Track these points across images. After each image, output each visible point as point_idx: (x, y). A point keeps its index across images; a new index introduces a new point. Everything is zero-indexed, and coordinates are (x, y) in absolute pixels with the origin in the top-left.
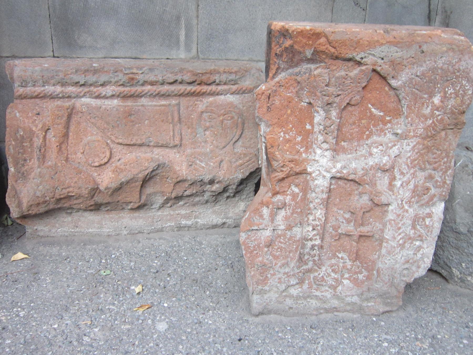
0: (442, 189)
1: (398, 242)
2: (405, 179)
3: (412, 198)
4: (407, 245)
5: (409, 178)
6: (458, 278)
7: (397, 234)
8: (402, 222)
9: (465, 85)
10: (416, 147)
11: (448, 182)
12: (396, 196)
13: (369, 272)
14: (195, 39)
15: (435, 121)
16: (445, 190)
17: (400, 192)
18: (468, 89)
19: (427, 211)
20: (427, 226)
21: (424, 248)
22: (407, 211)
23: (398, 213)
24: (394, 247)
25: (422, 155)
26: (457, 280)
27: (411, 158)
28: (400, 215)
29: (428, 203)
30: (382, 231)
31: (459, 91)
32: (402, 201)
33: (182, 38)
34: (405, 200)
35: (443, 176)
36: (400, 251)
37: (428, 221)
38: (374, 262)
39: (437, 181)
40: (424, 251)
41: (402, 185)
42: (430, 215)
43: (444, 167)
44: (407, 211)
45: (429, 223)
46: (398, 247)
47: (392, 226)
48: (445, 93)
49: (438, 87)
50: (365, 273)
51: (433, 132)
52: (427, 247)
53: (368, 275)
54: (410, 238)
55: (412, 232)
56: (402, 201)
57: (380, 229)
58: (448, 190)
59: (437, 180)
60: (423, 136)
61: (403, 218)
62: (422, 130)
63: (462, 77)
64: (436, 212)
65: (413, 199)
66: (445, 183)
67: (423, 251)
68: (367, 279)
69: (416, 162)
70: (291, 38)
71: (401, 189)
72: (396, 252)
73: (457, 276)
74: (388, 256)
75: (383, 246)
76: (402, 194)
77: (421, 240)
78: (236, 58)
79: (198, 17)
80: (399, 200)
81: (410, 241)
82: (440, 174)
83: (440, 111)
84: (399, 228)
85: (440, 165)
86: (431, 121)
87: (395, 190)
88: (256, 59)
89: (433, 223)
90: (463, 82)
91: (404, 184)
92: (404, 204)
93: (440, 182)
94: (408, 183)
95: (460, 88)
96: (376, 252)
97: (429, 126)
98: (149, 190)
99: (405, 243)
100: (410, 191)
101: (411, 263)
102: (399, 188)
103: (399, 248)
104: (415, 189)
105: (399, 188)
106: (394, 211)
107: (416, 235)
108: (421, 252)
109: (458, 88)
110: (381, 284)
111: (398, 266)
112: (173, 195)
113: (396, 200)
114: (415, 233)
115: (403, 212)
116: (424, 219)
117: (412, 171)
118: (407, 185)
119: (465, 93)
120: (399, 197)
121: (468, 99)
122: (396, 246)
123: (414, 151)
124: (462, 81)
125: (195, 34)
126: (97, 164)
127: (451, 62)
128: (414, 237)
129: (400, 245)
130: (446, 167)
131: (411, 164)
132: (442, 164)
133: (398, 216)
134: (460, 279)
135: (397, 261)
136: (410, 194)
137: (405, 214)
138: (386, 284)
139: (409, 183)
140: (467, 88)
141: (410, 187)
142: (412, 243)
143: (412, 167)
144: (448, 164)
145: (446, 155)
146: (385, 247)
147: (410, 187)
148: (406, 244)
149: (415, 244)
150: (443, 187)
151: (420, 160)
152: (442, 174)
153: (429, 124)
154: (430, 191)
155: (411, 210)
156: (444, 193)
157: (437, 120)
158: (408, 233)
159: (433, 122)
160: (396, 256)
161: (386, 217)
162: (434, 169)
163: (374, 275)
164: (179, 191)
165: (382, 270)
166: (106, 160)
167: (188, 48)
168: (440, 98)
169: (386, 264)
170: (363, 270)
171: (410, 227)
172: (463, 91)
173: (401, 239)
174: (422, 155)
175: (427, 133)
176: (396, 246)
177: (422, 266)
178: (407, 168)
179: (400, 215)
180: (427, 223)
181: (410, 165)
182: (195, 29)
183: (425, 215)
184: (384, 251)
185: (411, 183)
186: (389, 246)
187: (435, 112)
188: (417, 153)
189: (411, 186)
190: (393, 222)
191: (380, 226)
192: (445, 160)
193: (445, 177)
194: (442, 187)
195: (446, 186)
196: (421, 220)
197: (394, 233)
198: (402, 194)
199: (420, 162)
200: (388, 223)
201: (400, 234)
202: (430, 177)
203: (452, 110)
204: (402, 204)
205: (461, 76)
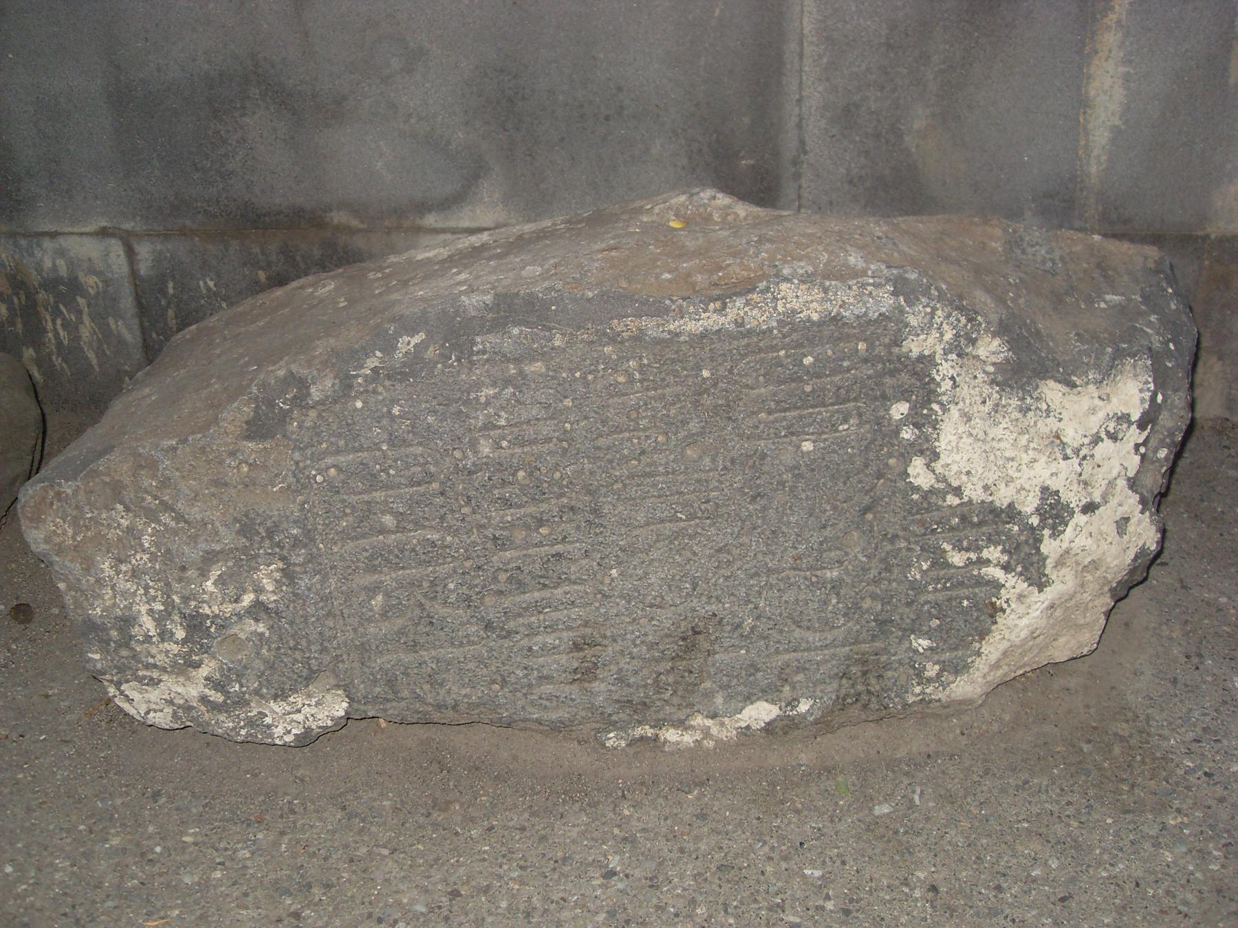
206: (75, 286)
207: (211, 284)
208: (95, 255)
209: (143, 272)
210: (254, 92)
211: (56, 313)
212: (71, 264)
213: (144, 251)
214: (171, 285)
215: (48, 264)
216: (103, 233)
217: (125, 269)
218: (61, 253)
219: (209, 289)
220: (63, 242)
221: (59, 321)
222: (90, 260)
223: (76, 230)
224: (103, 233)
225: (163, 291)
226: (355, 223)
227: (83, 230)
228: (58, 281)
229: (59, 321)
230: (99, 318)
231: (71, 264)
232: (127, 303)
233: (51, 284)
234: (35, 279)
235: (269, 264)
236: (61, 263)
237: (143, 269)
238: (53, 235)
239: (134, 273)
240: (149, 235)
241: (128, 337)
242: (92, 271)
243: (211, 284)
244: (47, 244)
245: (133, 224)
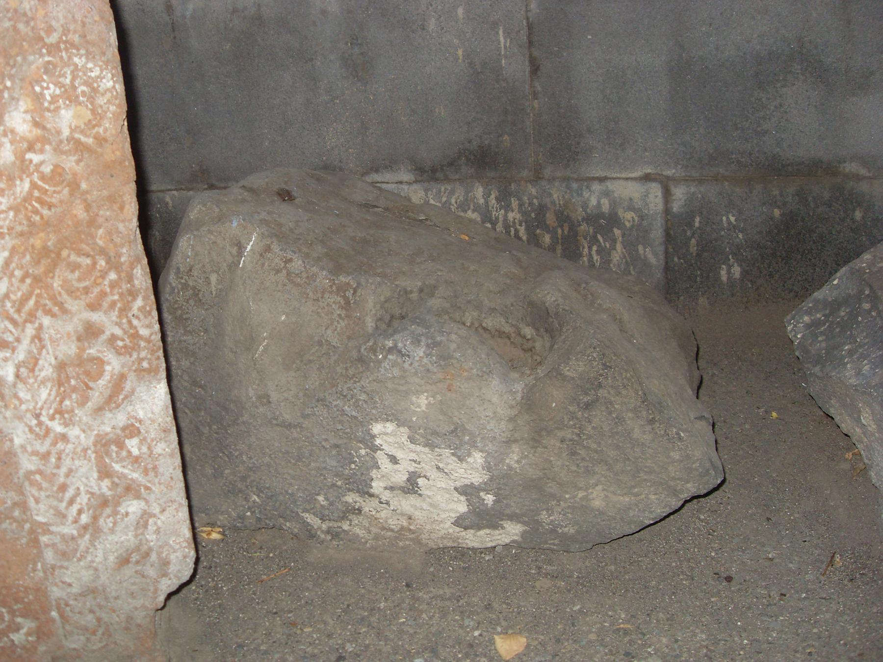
0: (135, 355)
1: (76, 521)
2: (21, 356)
3: (61, 402)
4: (106, 523)
5: (30, 352)
6: (322, 532)
7: (64, 504)
8: (64, 470)
9: (84, 66)
10: (13, 265)
11: (144, 332)
12: (15, 408)
13: (37, 619)
15: (40, 183)
16: (143, 354)
17: (21, 395)
18: (100, 78)
19: (121, 419)
20: (137, 460)
21: (155, 516)
22: (64, 438)
23: (43, 449)
24: (73, 538)
25: (37, 280)
26: (323, 536)
27: (12, 297)
28: (48, 453)
29: (110, 399)
30: (23, 506)
31: (75, 88)
32: (38, 416)
34: (44, 413)
35: (124, 321)
36: (92, 542)
37: (133, 444)
38: (40, 591)
39: (113, 338)
40: (159, 522)
41: (17, 376)
42: (131, 430)
43: (116, 297)
44: (64, 438)
45: (140, 449)
46: (81, 536)
47: (40, 489)
48: (38, 98)
49: (6, 88)
50: (27, 625)
51: (45, 212)
52: (163, 511)
53: (39, 628)
54: (104, 503)
55: (106, 483)
56: (38, 416)
57: (15, 504)
58: (153, 352)
59: (113, 335)
60: (19, 228)
61: (59, 459)
62: (12, 214)
63: (66, 50)
64: (150, 415)
65: (67, 403)
66: (136, 336)
67: (155, 523)
68: (38, 638)
69: (31, 303)
71: (20, 385)
72: (82, 547)
73: (320, 528)
74: (66, 564)
75: (42, 545)
76: (29, 397)
77: (138, 497)
80: (29, 415)
81: (108, 511)
82: (114, 318)
83: (42, 151)
84: (63, 488)
85: (103, 294)
86: (27, 185)
87: (6, 391)
89: (149, 448)
90: (76, 60)
91: (23, 370)
92: (50, 423)
93: (123, 340)
94: (32, 364)
95: (74, 78)
96: (35, 564)
97: (25, 200)
99: (95, 518)
100: (49, 385)
101: (138, 562)
102: (15, 385)
103: (87, 537)
104: (59, 376)
105: (15, 385)
106: (29, 449)
107: (120, 490)
108: (151, 528)
109: (68, 81)
110: (82, 638)
111: (103, 579)
113: (20, 418)
114: (115, 485)
115: (55, 443)
116: (121, 445)
117: (30, 330)
118: (32, 370)
119: (95, 90)
120: (24, 407)
121: (109, 102)
122: (75, 532)
123: (12, 275)
124: (70, 58)
127: (16, 11)
128: (114, 497)
129: (85, 528)
130: (121, 295)
131: (19, 311)
132: (108, 290)
133: (45, 456)
134: (328, 532)
135: (96, 569)
136: (54, 393)
137: (60, 446)
138: (94, 633)
139: (36, 364)
140: (93, 75)
141: (43, 374)
142: (115, 513)
143: (26, 321)
144: (125, 286)
145: (107, 262)
146: (47, 546)
147: (43, 374)
148: (101, 521)
149: (127, 514)
150: (135, 347)
151: (38, 296)
152: (120, 317)
153: (24, 193)
154: (108, 368)
155: (74, 432)
156: (145, 365)
157: (43, 178)
158: (95, 489)
159: (34, 185)
160: (89, 558)
161: (17, 470)
162: (93, 307)
163: (53, 620)
165: (67, 605)
168: (28, 117)
169: (70, 585)
170: (19, 620)
171: (95, 475)
172: (86, 83)
173: (80, 512)
174: (37, 280)
175: (29, 219)
176: (75, 532)
177: (173, 557)
178: (11, 327)
179: (48, 453)
180: (135, 452)
181: (16, 316)
183: (119, 431)
184: (49, 555)
185: (40, 362)
186: (57, 539)
187: (29, 156)
188: (22, 280)
189: (46, 370)
190: (38, 477)
191: (11, 497)
192: (113, 276)
193: (130, 322)
194: (133, 349)
195: (143, 344)
196: (114, 448)
197: (55, 503)
198: (29, 397)
199: (43, 302)
200: (27, 484)
201: (71, 502)
202: (91, 332)
203: (78, 142)
204: (40, 424)
205: (62, 46)
206: (613, 220)
207: (732, 219)
208: (636, 196)
209: (675, 209)
210: (796, 67)
211: (594, 240)
212: (614, 204)
213: (679, 193)
214: (697, 219)
215: (593, 202)
216: (647, 178)
217: (660, 207)
218: (607, 194)
219: (729, 222)
220: (609, 185)
221: (595, 248)
222: (631, 199)
223: (623, 175)
224: (647, 178)
225: (690, 225)
226: (863, 172)
227: (630, 175)
228: (601, 215)
229: (595, 248)
230: (630, 245)
231: (614, 204)
232: (657, 234)
233: (593, 218)
234: (579, 214)
235: (785, 204)
236: (605, 202)
237: (676, 207)
238: (602, 180)
239: (667, 211)
240: (686, 180)
241: (653, 260)
242: (631, 208)
243: (732, 219)
244: (596, 187)
245: (674, 171)
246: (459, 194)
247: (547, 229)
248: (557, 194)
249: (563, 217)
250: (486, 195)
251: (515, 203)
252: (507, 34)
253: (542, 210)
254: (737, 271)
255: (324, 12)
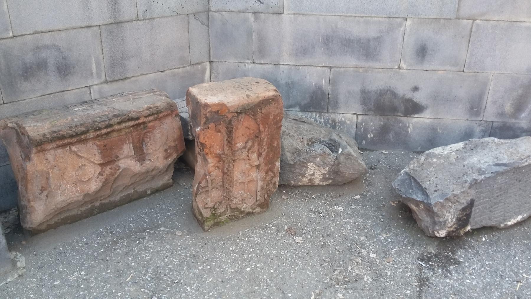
14: (103, 69)
33: (94, 70)
70: (210, 107)
78: (132, 75)
79: (103, 54)
88: (145, 73)
98: (114, 186)
112: (130, 184)
125: (103, 65)
126: (87, 179)
164: (133, 180)
166: (92, 175)
167: (99, 75)
182: (102, 63)
212: (345, 119)
213: (360, 117)
216: (355, 114)
224: (355, 114)
225: (362, 125)
231: (345, 119)
234: (337, 121)
237: (359, 121)
244: (341, 115)
246: (310, 114)
247: (329, 123)
248: (333, 116)
249: (334, 121)
250: (316, 115)
251: (322, 117)
252: (325, 80)
253: (328, 119)
254: (372, 135)
255: (283, 72)
